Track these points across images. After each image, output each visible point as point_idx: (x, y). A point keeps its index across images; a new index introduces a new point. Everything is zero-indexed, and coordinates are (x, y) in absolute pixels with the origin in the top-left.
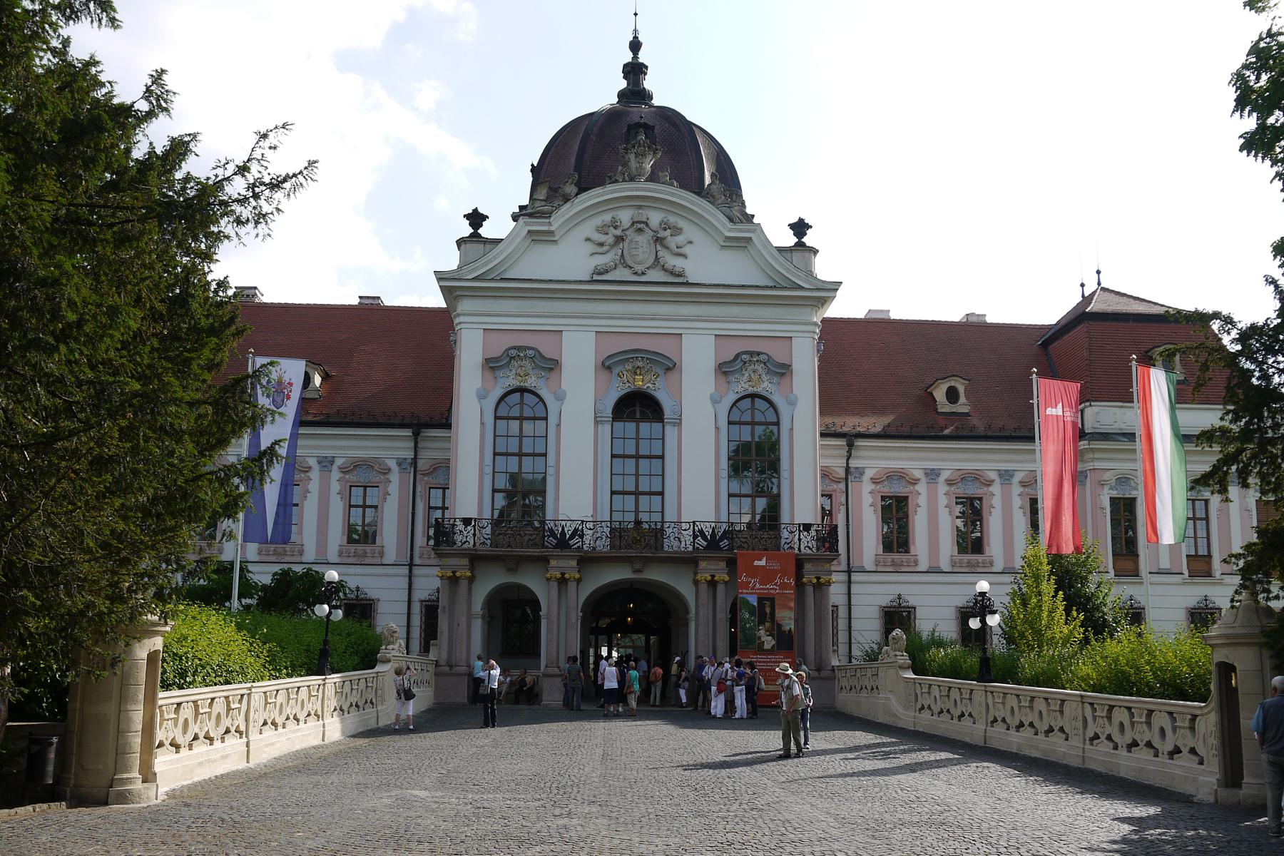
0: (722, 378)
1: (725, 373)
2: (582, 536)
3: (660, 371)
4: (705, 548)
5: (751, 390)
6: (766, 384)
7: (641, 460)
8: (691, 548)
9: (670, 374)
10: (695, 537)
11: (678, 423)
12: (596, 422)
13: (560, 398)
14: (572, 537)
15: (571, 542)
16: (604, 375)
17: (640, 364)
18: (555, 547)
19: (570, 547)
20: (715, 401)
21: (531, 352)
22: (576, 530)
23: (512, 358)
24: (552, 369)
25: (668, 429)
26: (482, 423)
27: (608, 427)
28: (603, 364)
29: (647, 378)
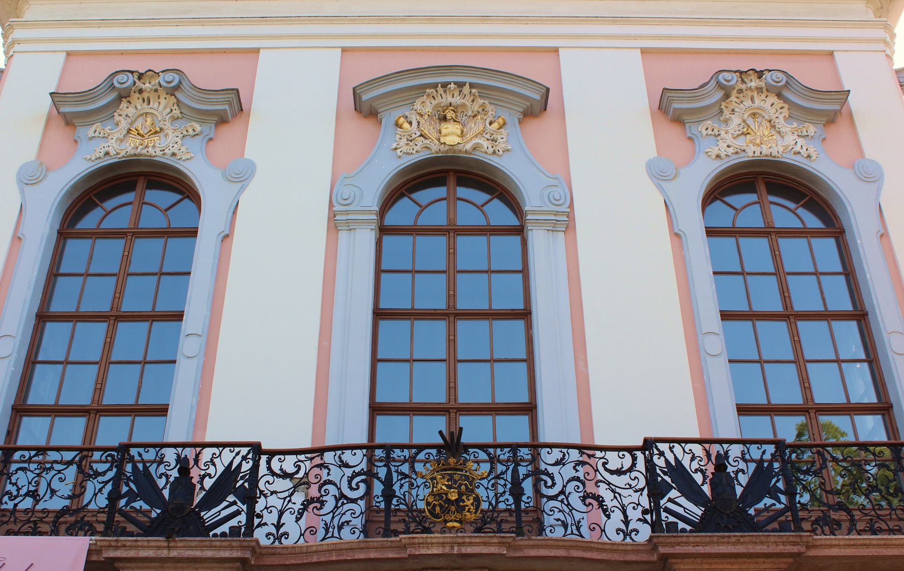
0: (672, 132)
1: (678, 119)
2: (250, 497)
3: (510, 116)
4: (700, 526)
5: (752, 152)
6: (790, 139)
7: (463, 326)
8: (645, 533)
9: (533, 125)
10: (656, 490)
11: (565, 222)
12: (337, 222)
13: (241, 176)
14: (214, 497)
15: (208, 515)
16: (359, 127)
17: (457, 100)
18: (151, 529)
19: (203, 530)
20: (659, 175)
21: (169, 77)
22: (230, 473)
23: (123, 96)
24: (222, 120)
25: (537, 238)
26: (17, 239)
27: (366, 238)
28: (358, 106)
29: (475, 127)
